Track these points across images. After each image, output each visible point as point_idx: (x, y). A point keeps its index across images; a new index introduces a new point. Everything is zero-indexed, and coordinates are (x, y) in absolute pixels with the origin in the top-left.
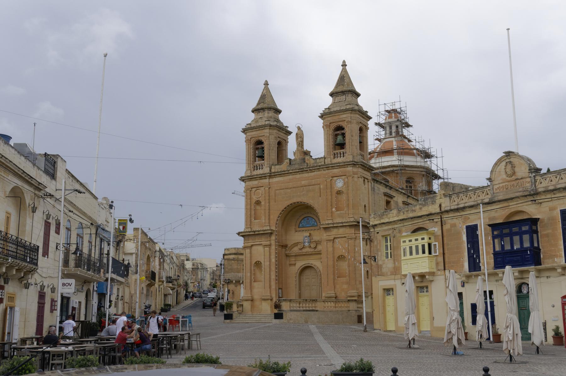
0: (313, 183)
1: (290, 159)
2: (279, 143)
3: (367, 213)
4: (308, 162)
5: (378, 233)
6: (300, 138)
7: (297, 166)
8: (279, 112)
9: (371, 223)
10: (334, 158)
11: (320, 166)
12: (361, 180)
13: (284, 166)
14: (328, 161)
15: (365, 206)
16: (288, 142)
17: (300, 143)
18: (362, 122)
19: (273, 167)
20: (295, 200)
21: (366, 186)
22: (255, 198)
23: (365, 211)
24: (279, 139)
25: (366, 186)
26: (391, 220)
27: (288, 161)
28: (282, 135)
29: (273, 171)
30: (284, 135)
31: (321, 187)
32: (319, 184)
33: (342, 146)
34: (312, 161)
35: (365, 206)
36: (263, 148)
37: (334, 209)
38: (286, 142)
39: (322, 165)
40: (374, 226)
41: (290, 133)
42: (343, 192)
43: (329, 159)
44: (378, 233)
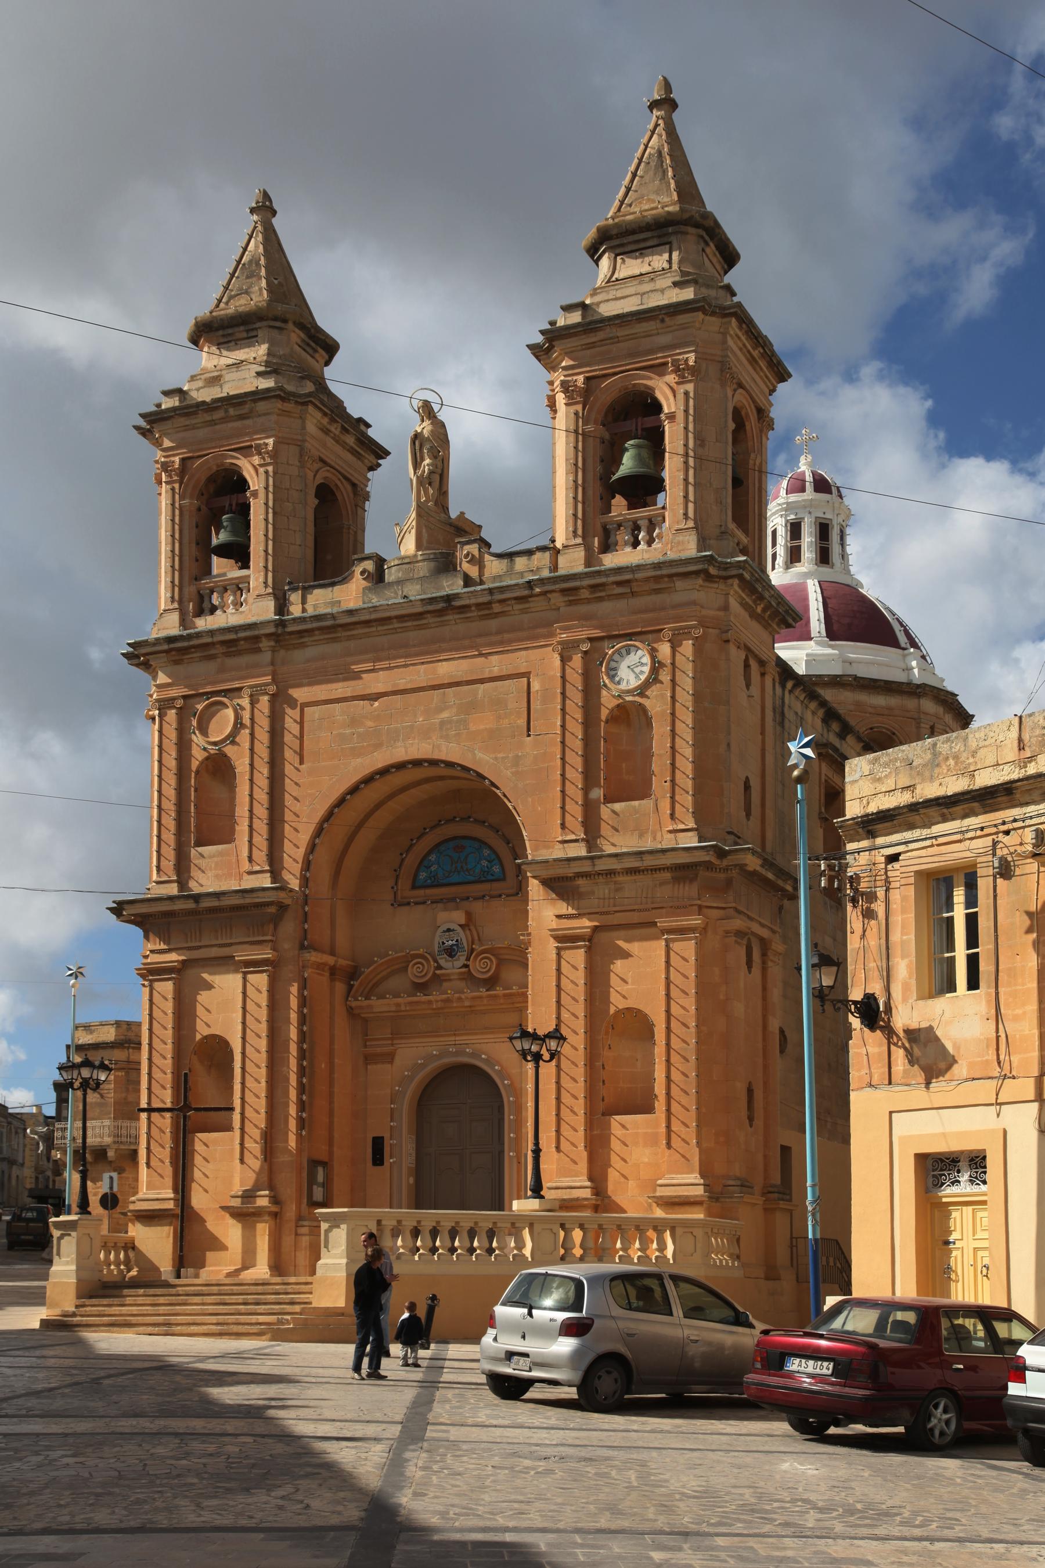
0: (496, 671)
1: (380, 562)
2: (325, 493)
3: (755, 822)
4: (473, 572)
5: (893, 858)
6: (433, 445)
7: (414, 592)
8: (330, 348)
9: (853, 809)
10: (607, 547)
11: (530, 584)
12: (737, 656)
13: (351, 594)
14: (573, 562)
15: (747, 787)
16: (366, 497)
17: (437, 480)
18: (746, 379)
19: (295, 597)
20: (401, 752)
21: (755, 690)
22: (199, 746)
23: (748, 815)
24: (323, 475)
25: (755, 690)
26: (986, 778)
27: (369, 565)
28: (340, 457)
29: (295, 611)
30: (349, 457)
31: (536, 686)
32: (526, 675)
33: (644, 488)
34: (494, 567)
35: (747, 787)
36: (244, 510)
37: (597, 793)
38: (360, 495)
39: (542, 581)
40: (874, 824)
41: (381, 453)
42: (642, 709)
43: (580, 554)
44: (893, 858)
